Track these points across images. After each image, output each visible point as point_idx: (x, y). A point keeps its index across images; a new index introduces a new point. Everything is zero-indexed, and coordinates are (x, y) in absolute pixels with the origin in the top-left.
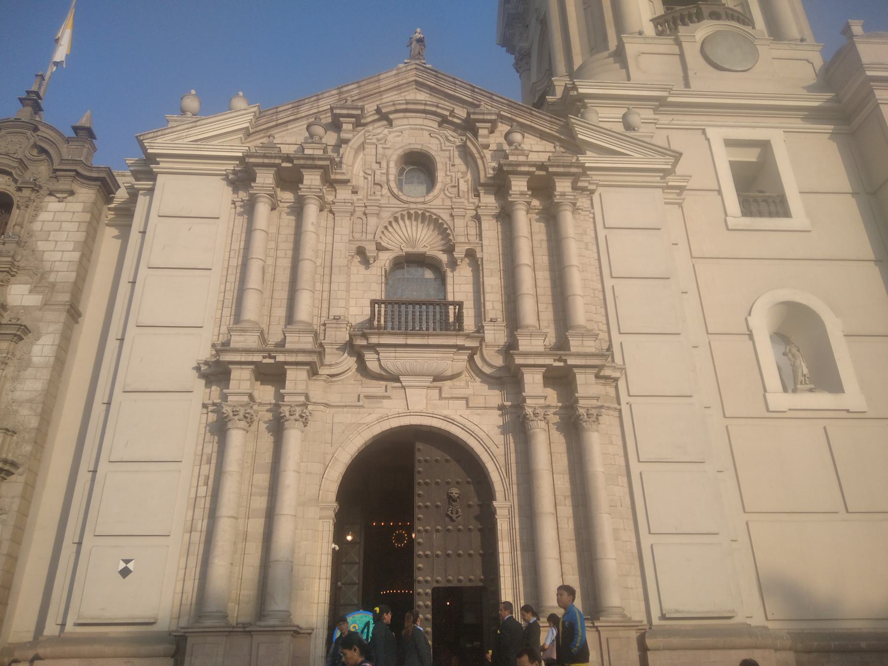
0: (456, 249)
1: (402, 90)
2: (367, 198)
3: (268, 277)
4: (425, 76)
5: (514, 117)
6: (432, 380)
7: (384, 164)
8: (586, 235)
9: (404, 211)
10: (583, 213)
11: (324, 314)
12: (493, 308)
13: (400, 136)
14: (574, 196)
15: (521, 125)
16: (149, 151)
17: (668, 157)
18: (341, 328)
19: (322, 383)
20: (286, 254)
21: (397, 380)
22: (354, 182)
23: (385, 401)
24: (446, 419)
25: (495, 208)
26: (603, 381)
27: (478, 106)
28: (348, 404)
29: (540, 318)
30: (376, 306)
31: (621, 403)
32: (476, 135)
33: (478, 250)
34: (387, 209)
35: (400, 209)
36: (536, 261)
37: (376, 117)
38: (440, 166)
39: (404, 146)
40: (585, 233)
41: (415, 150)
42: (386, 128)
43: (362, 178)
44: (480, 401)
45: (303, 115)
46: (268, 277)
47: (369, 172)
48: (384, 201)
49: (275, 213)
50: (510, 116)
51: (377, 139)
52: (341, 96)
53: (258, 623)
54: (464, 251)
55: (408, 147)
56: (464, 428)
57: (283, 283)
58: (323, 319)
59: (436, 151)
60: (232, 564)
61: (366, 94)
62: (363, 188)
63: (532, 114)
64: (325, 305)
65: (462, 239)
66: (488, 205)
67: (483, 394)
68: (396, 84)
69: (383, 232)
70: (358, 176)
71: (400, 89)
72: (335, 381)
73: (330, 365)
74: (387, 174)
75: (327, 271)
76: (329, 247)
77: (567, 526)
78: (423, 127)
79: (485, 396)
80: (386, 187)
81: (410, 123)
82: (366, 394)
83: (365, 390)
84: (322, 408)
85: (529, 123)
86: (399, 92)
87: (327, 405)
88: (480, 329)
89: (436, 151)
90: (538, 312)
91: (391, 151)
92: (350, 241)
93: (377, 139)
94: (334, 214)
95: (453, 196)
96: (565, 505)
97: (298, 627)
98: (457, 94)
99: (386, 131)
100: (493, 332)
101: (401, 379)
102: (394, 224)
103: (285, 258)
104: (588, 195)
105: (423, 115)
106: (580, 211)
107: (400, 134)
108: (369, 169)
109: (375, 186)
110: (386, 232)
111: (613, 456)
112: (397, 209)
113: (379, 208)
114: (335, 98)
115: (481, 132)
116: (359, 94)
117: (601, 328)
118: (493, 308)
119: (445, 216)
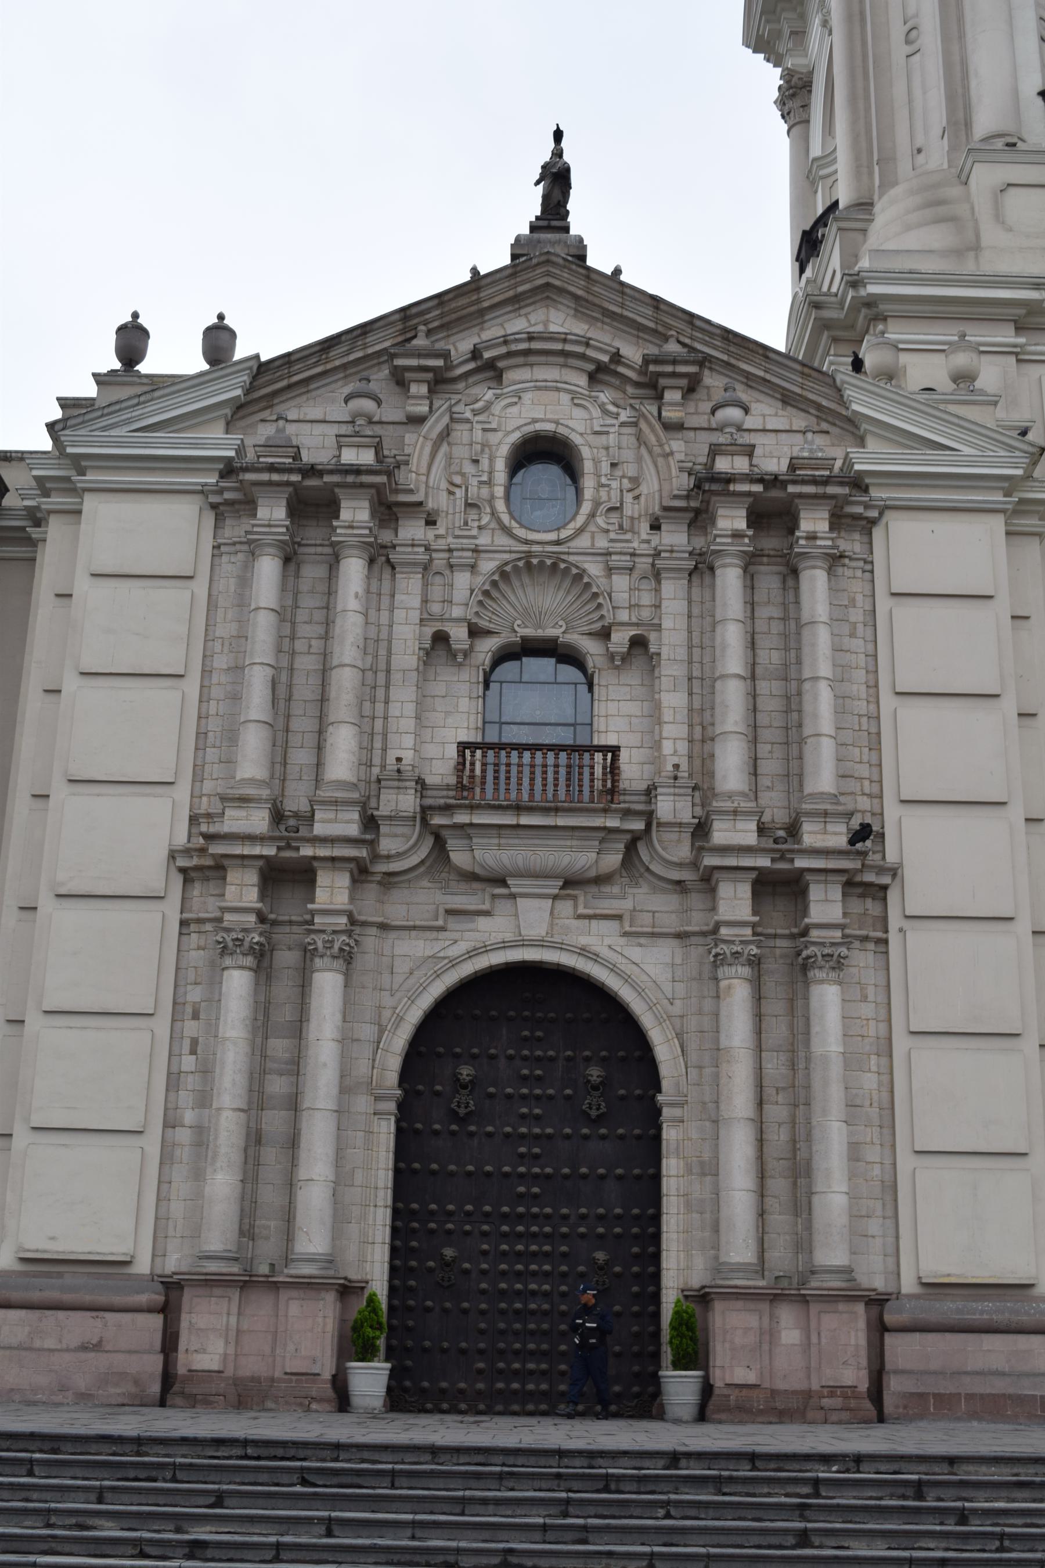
0: (613, 635)
1: (522, 304)
2: (453, 533)
3: (282, 691)
4: (566, 275)
5: (733, 361)
6: (561, 883)
7: (485, 463)
8: (855, 607)
9: (519, 559)
10: (854, 564)
11: (377, 761)
12: (675, 751)
13: (516, 403)
14: (832, 539)
15: (748, 375)
16: (69, 450)
17: (1018, 454)
18: (406, 788)
19: (374, 885)
20: (310, 646)
21: (502, 882)
22: (430, 505)
23: (482, 922)
24: (584, 952)
25: (687, 555)
26: (860, 890)
27: (666, 339)
28: (418, 923)
29: (759, 772)
30: (468, 752)
31: (890, 929)
32: (660, 397)
33: (652, 637)
34: (491, 555)
35: (514, 556)
36: (758, 660)
37: (471, 366)
38: (588, 466)
39: (522, 426)
40: (853, 602)
41: (543, 433)
42: (489, 388)
43: (445, 494)
44: (645, 922)
45: (337, 363)
46: (282, 691)
47: (457, 480)
48: (484, 540)
49: (292, 567)
50: (725, 358)
51: (473, 410)
52: (407, 324)
53: (286, 1271)
54: (628, 638)
55: (530, 428)
56: (613, 969)
57: (305, 701)
58: (376, 771)
59: (581, 434)
60: (242, 1181)
61: (454, 316)
62: (447, 513)
63: (767, 357)
64: (378, 745)
65: (624, 616)
66: (675, 548)
67: (650, 909)
68: (511, 293)
69: (480, 603)
70: (438, 489)
71: (518, 301)
72: (395, 883)
73: (388, 857)
74: (489, 483)
75: (381, 677)
76: (384, 635)
77: (776, 1138)
78: (559, 385)
79: (654, 912)
80: (488, 510)
81: (534, 378)
82: (449, 907)
83: (448, 898)
84: (374, 931)
85: (761, 374)
86: (517, 306)
87: (384, 927)
88: (650, 792)
89: (581, 434)
90: (756, 759)
91: (500, 434)
92: (421, 620)
93: (473, 410)
94: (393, 568)
95: (610, 528)
96: (777, 1103)
97: (345, 1278)
98: (626, 313)
99: (489, 395)
100: (672, 798)
101: (509, 882)
102: (502, 586)
103: (309, 653)
104: (863, 528)
105: (561, 360)
106: (847, 561)
107: (515, 400)
108: (457, 473)
109: (468, 509)
110: (488, 602)
111: (865, 1022)
112: (507, 557)
113: (475, 555)
114: (398, 328)
115: (671, 396)
116: (441, 316)
117: (867, 791)
118: (675, 753)
119: (594, 569)
